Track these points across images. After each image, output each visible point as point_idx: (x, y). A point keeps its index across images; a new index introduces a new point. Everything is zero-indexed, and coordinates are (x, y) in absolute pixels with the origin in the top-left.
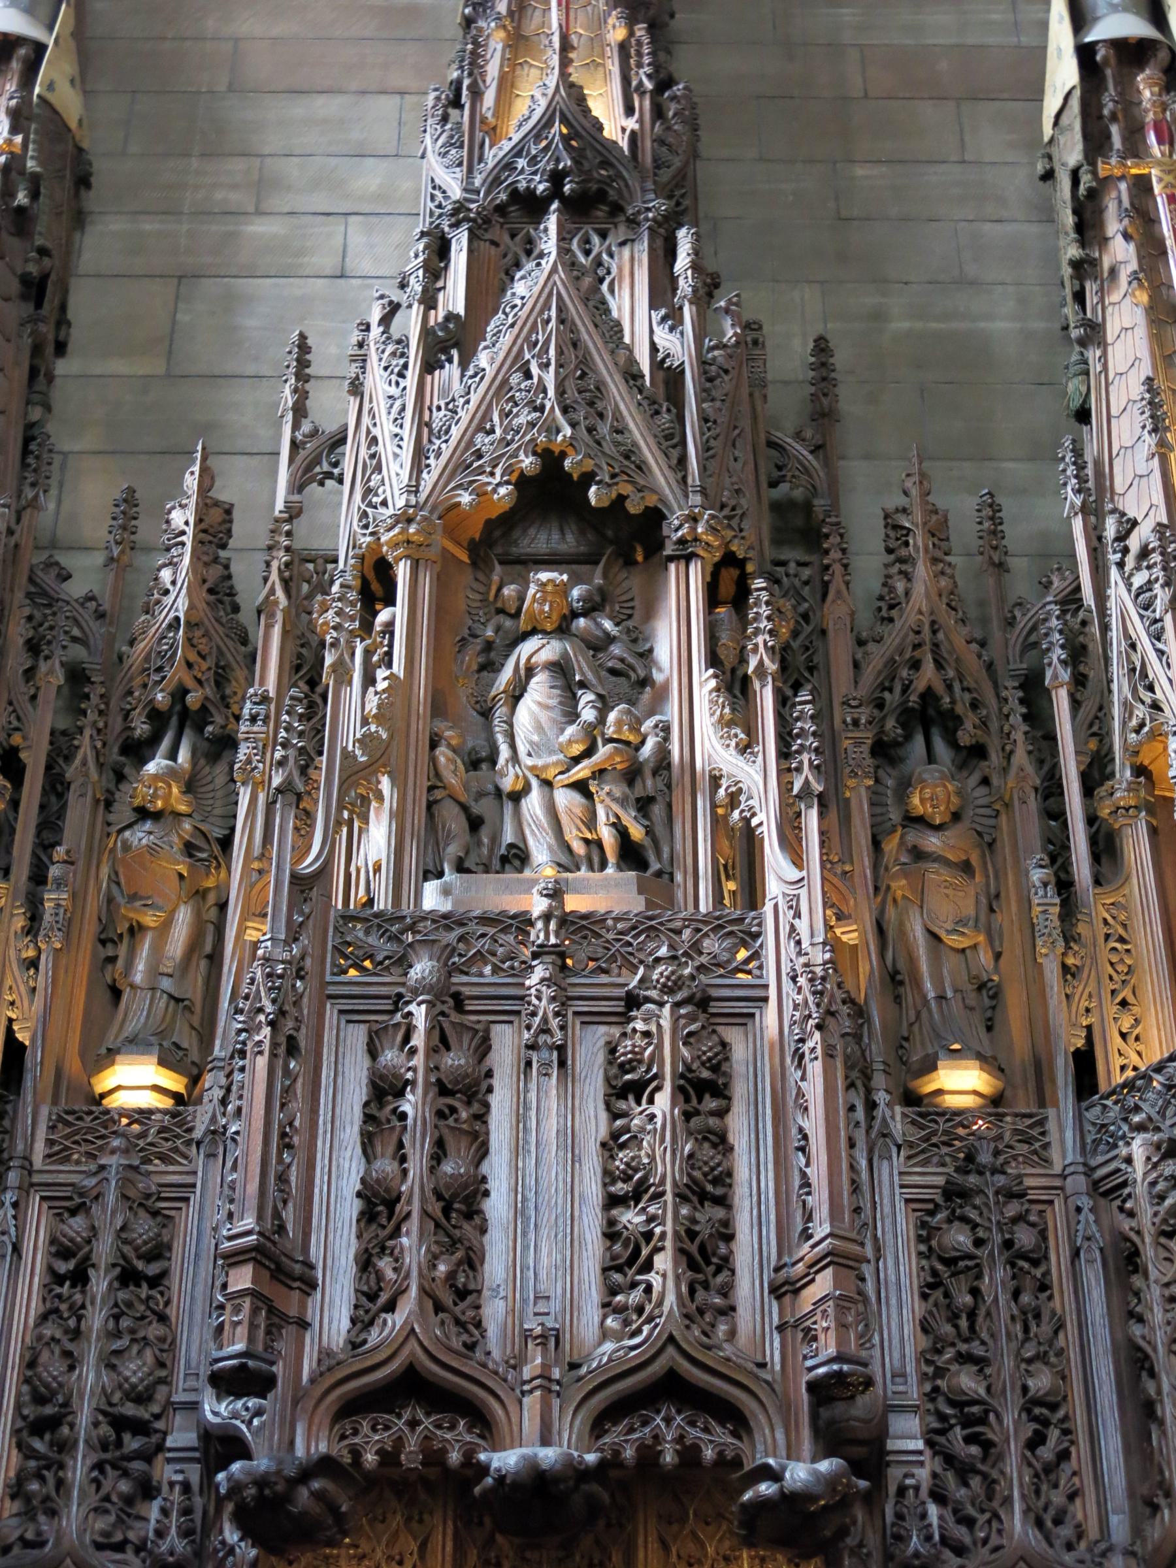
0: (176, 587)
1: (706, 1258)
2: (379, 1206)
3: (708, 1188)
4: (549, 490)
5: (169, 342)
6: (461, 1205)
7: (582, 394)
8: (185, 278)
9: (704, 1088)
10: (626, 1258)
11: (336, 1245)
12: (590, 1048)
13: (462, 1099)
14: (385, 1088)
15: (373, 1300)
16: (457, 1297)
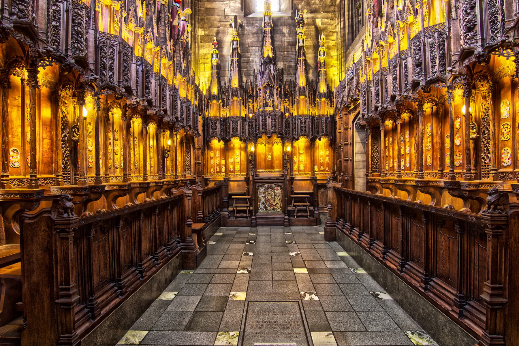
0: (250, 86)
1: (275, 127)
2: (262, 125)
3: (276, 124)
4: (268, 85)
5: (247, 68)
6: (266, 124)
7: (270, 79)
8: (247, 63)
9: (275, 119)
10: (272, 127)
11: (261, 126)
12: (271, 117)
13: (266, 119)
14: (262, 119)
15: (262, 129)
16: (266, 129)
